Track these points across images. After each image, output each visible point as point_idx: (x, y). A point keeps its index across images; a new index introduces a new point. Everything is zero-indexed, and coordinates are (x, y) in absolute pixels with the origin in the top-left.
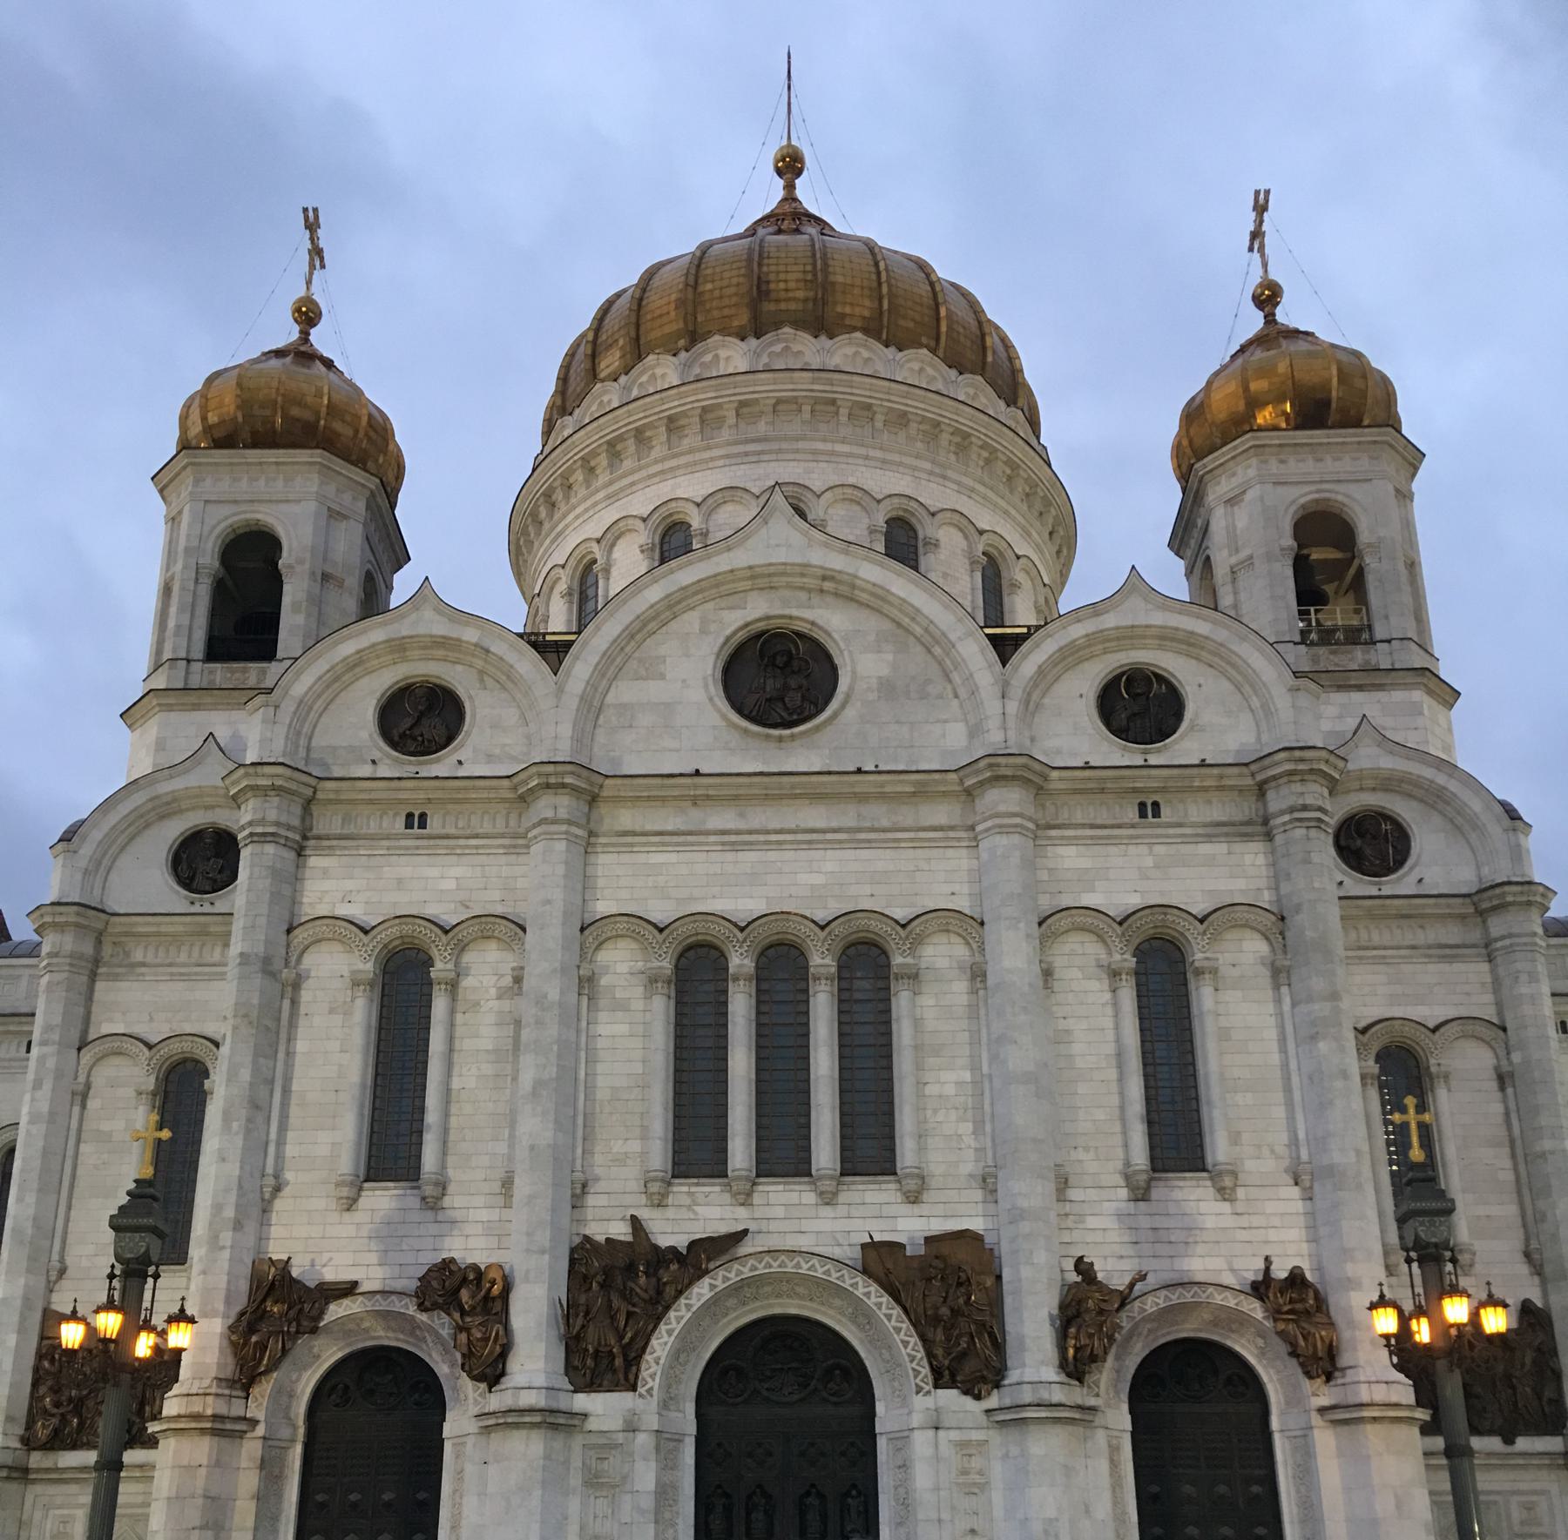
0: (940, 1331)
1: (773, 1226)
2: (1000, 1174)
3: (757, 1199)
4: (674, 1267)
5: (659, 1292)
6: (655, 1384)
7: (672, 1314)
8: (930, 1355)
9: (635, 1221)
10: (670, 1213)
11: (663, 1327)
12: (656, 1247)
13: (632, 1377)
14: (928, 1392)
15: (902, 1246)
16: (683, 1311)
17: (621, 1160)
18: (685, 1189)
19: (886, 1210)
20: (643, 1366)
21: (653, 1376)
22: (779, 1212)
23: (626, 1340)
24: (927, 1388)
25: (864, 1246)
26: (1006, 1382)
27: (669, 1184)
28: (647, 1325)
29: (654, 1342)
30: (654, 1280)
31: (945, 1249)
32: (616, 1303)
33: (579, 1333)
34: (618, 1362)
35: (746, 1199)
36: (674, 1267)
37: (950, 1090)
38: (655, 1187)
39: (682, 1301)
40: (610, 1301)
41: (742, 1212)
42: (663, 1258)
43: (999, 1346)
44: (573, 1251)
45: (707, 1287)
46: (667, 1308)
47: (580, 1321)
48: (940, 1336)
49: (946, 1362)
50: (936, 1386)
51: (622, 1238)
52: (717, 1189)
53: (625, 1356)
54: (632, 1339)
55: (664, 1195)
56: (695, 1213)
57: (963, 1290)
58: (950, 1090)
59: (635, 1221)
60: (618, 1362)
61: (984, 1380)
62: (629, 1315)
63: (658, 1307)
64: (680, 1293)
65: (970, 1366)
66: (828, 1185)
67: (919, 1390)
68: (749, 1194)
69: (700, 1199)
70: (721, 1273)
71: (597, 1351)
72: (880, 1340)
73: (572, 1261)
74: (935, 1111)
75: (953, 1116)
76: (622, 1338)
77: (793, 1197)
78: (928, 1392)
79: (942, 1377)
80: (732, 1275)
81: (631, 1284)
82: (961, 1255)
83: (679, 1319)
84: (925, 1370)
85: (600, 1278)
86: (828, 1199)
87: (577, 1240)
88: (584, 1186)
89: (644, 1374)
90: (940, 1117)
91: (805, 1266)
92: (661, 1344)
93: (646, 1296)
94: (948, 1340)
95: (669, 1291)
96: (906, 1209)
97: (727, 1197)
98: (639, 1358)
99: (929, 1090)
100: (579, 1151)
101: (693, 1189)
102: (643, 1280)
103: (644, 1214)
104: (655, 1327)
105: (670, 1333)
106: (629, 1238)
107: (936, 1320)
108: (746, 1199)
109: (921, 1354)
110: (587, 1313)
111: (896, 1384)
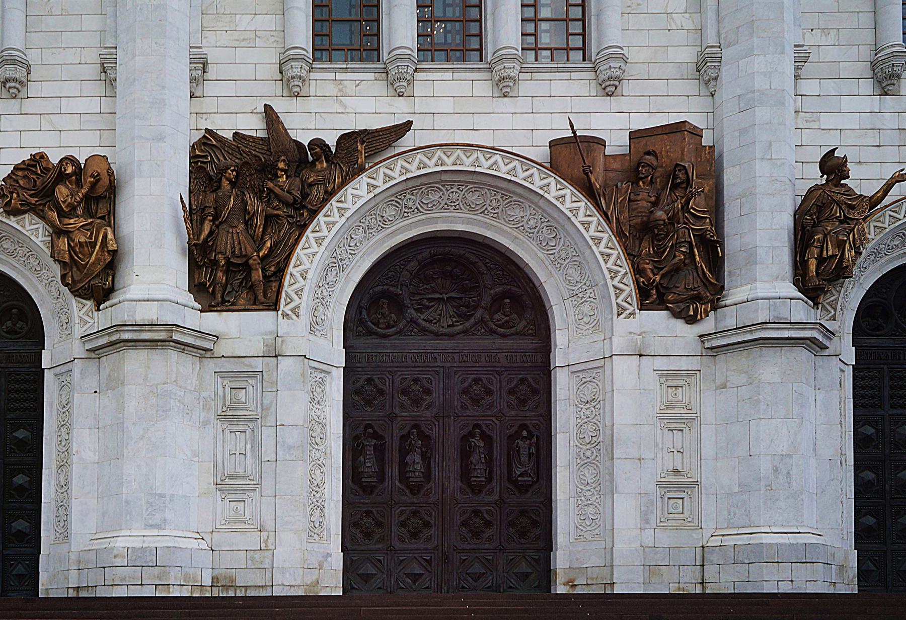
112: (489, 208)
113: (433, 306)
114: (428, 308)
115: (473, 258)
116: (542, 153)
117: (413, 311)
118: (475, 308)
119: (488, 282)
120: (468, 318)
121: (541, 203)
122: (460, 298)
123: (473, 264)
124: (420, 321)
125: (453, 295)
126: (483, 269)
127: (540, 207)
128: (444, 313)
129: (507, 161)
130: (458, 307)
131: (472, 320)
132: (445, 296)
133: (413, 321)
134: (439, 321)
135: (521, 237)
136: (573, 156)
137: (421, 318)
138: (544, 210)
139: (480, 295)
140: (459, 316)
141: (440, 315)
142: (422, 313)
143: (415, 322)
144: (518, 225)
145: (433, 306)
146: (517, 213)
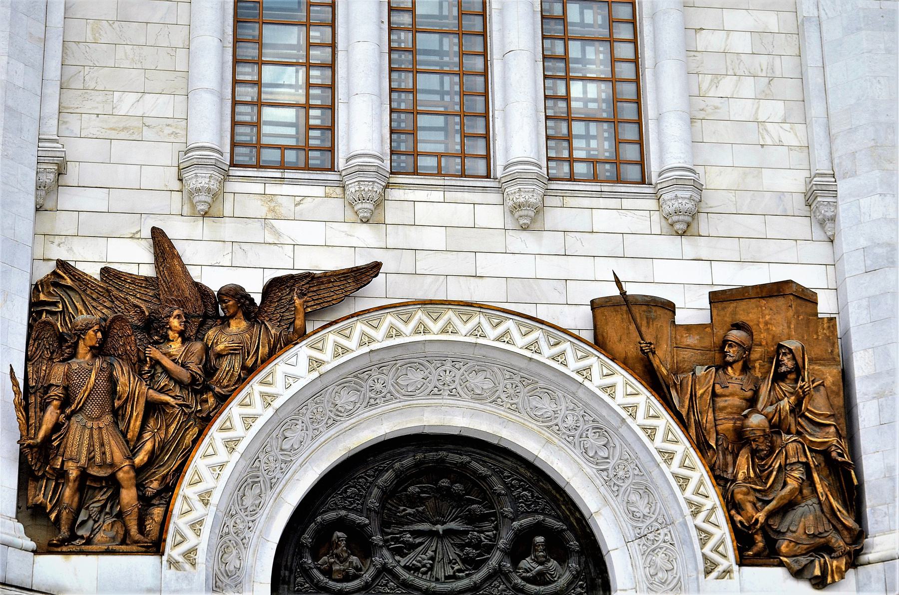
0: (743, 460)
1: (425, 263)
2: (842, 187)
3: (392, 212)
4: (238, 326)
5: (209, 371)
6: (203, 542)
7: (234, 410)
8: (731, 504)
9: (161, 244)
10: (228, 229)
11: (215, 435)
12: (202, 291)
13: (152, 526)
14: (727, 572)
15: (669, 307)
16: (258, 407)
17: (134, 130)
18: (258, 188)
19: (635, 246)
20: (178, 506)
21: (196, 526)
22: (435, 238)
23: (141, 458)
24: (724, 564)
25: (596, 305)
26: (870, 557)
27: (227, 177)
28: (182, 429)
29: (199, 463)
30: (198, 346)
31: (748, 313)
32: (126, 381)
33: (48, 439)
34: (128, 495)
35: (372, 213)
36: (238, 326)
37: (741, 43)
38: (203, 179)
39: (255, 387)
40: (113, 382)
41: (365, 235)
42: (213, 307)
43: (852, 495)
44: (36, 289)
45: (304, 363)
46: (223, 400)
47: (50, 416)
48: (743, 467)
49: (761, 516)
50: (743, 561)
51: (133, 270)
52: (319, 191)
53: (140, 486)
54: (153, 457)
55: (217, 196)
56: (277, 233)
57: (786, 387)
58: (741, 43)
59: (161, 244)
60: (128, 495)
61: (827, 549)
62: (153, 408)
63: (208, 392)
64: (250, 371)
65: (804, 522)
66: (530, 194)
67: (710, 567)
68: (379, 203)
69: (286, 205)
70: (331, 338)
71: (84, 475)
72: (630, 479)
73: (36, 307)
74: (717, 77)
75: (748, 87)
76: (134, 453)
77: (461, 214)
78: (727, 572)
79: (755, 546)
80: (352, 344)
81: (154, 352)
82: (775, 323)
83: (249, 420)
84: (722, 532)
85: (93, 337)
86: (528, 218)
87: (45, 270)
88: (60, 172)
89: (179, 522)
90: (727, 86)
91: (492, 333)
92: (213, 467)
93: (185, 375)
94: (762, 477)
95: (229, 366)
96: (670, 245)
97: (335, 207)
98: (168, 490)
99: (704, 41)
100: (52, 106)
101: (271, 189)
102: (176, 347)
103: (175, 230)
104: (201, 434)
105: (231, 445)
106: (148, 271)
107: (741, 438)
108: (372, 213)
109: (713, 498)
110: (66, 402)
111: (660, 559)
112: (503, 396)
113: (420, 544)
114: (412, 547)
115: (483, 470)
116: (579, 319)
117: (385, 552)
118: (489, 549)
119: (508, 510)
120: (477, 565)
121: (581, 393)
122: (466, 532)
123: (484, 478)
124: (399, 570)
125: (453, 525)
126: (499, 488)
127: (580, 400)
128: (439, 557)
129: (524, 330)
130: (462, 547)
131: (483, 572)
132: (440, 528)
133: (385, 570)
134: (431, 569)
135: (556, 441)
136: (627, 325)
137: (397, 564)
138: (586, 405)
139: (496, 528)
140: (465, 561)
141: (432, 558)
142: (403, 555)
143: (391, 572)
144: (549, 422)
145: (420, 544)
146: (546, 406)
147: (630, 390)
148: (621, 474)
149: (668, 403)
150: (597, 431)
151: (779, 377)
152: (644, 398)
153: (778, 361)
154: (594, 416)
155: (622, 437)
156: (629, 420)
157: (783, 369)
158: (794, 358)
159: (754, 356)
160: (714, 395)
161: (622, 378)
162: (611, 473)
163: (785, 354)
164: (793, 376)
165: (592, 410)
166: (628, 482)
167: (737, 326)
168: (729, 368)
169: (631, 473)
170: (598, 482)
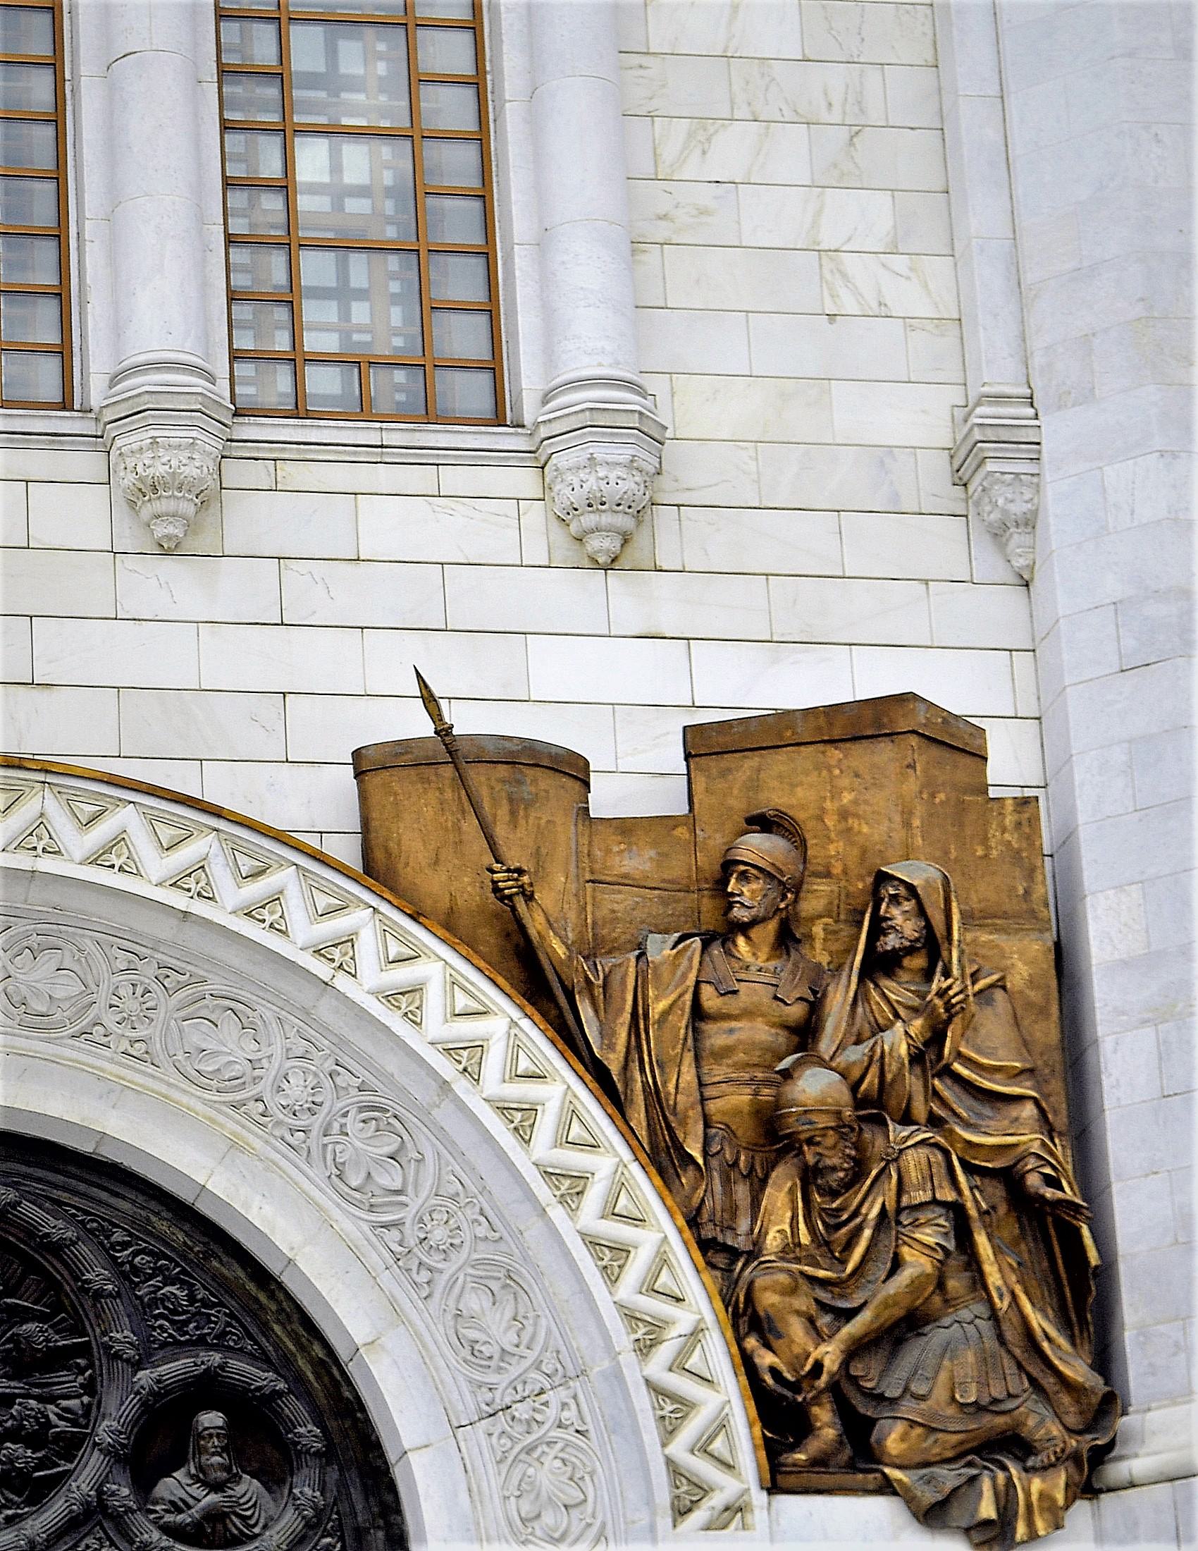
0: (780, 1196)
8: (747, 1320)
14: (736, 1509)
15: (574, 770)
19: (476, 598)
24: (726, 1488)
31: (791, 783)
43: (1083, 1291)
48: (780, 1215)
49: (830, 1354)
57: (897, 990)
61: (1014, 1445)
65: (948, 1373)
66: (183, 453)
67: (687, 1497)
82: (867, 813)
84: (724, 1399)
86: (178, 522)
91: (80, 843)
94: (831, 1245)
107: (774, 1135)
109: (696, 1303)
111: (547, 1474)
112: (110, 1019)
116: (323, 803)
119: (123, 1336)
121: (325, 1010)
123: (56, 1248)
126: (98, 1274)
127: (325, 1030)
129: (166, 833)
135: (258, 1144)
136: (458, 821)
138: (341, 1043)
144: (237, 1092)
146: (230, 1046)
147: (462, 1002)
148: (439, 1235)
149: (569, 1037)
150: (373, 1116)
151: (880, 965)
152: (505, 1023)
153: (877, 920)
154: (365, 1075)
155: (440, 1133)
156: (461, 1086)
157: (891, 942)
158: (921, 911)
159: (810, 905)
160: (698, 1013)
161: (439, 967)
162: (412, 1234)
163: (895, 899)
164: (918, 962)
165: (359, 1057)
166: (458, 1258)
167: (763, 823)
168: (741, 941)
169: (466, 1235)
170: (374, 1259)
